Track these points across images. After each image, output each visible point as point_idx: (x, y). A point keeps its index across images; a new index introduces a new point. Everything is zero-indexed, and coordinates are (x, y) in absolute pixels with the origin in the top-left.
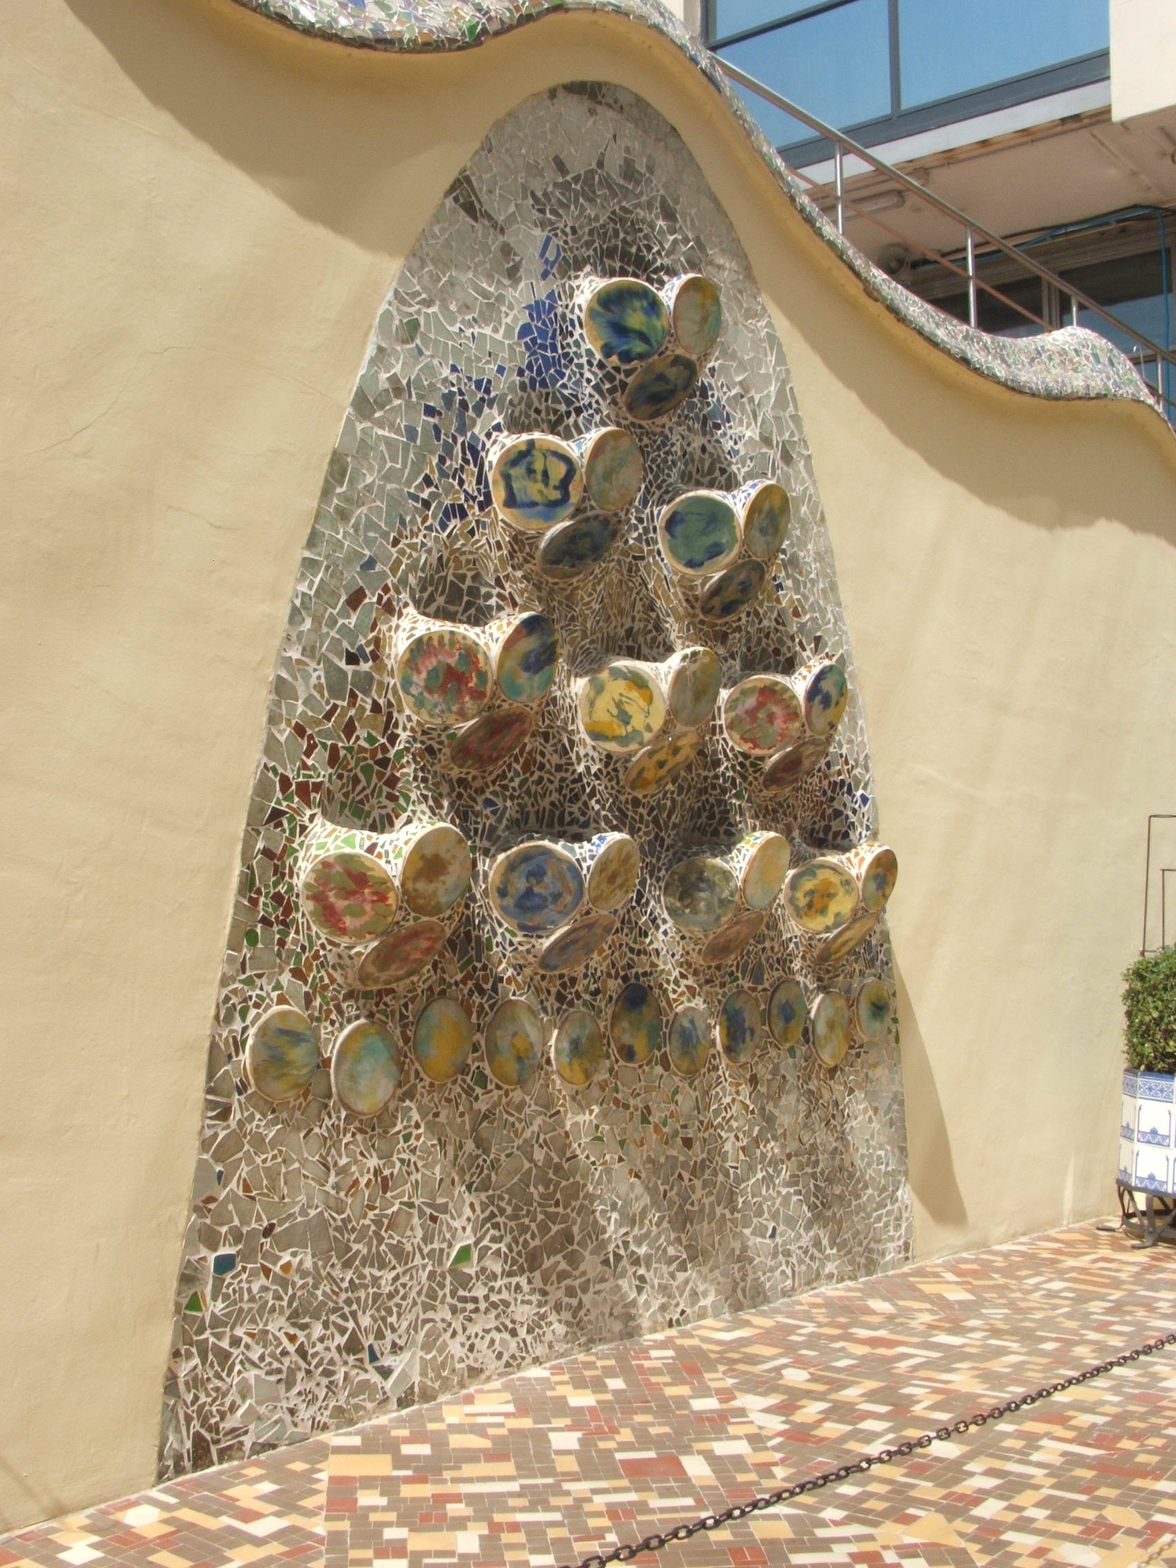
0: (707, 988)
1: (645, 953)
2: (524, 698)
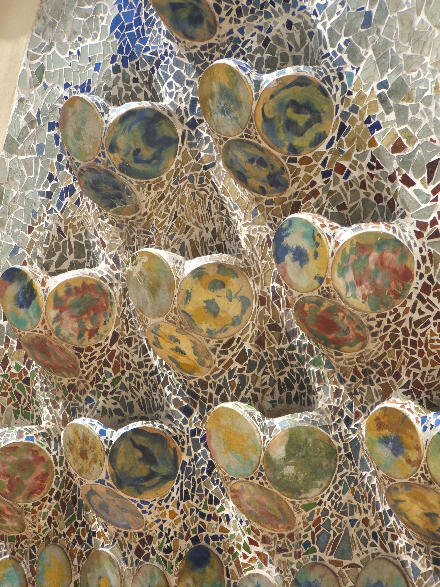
0: (279, 556)
1: (215, 518)
2: (29, 326)
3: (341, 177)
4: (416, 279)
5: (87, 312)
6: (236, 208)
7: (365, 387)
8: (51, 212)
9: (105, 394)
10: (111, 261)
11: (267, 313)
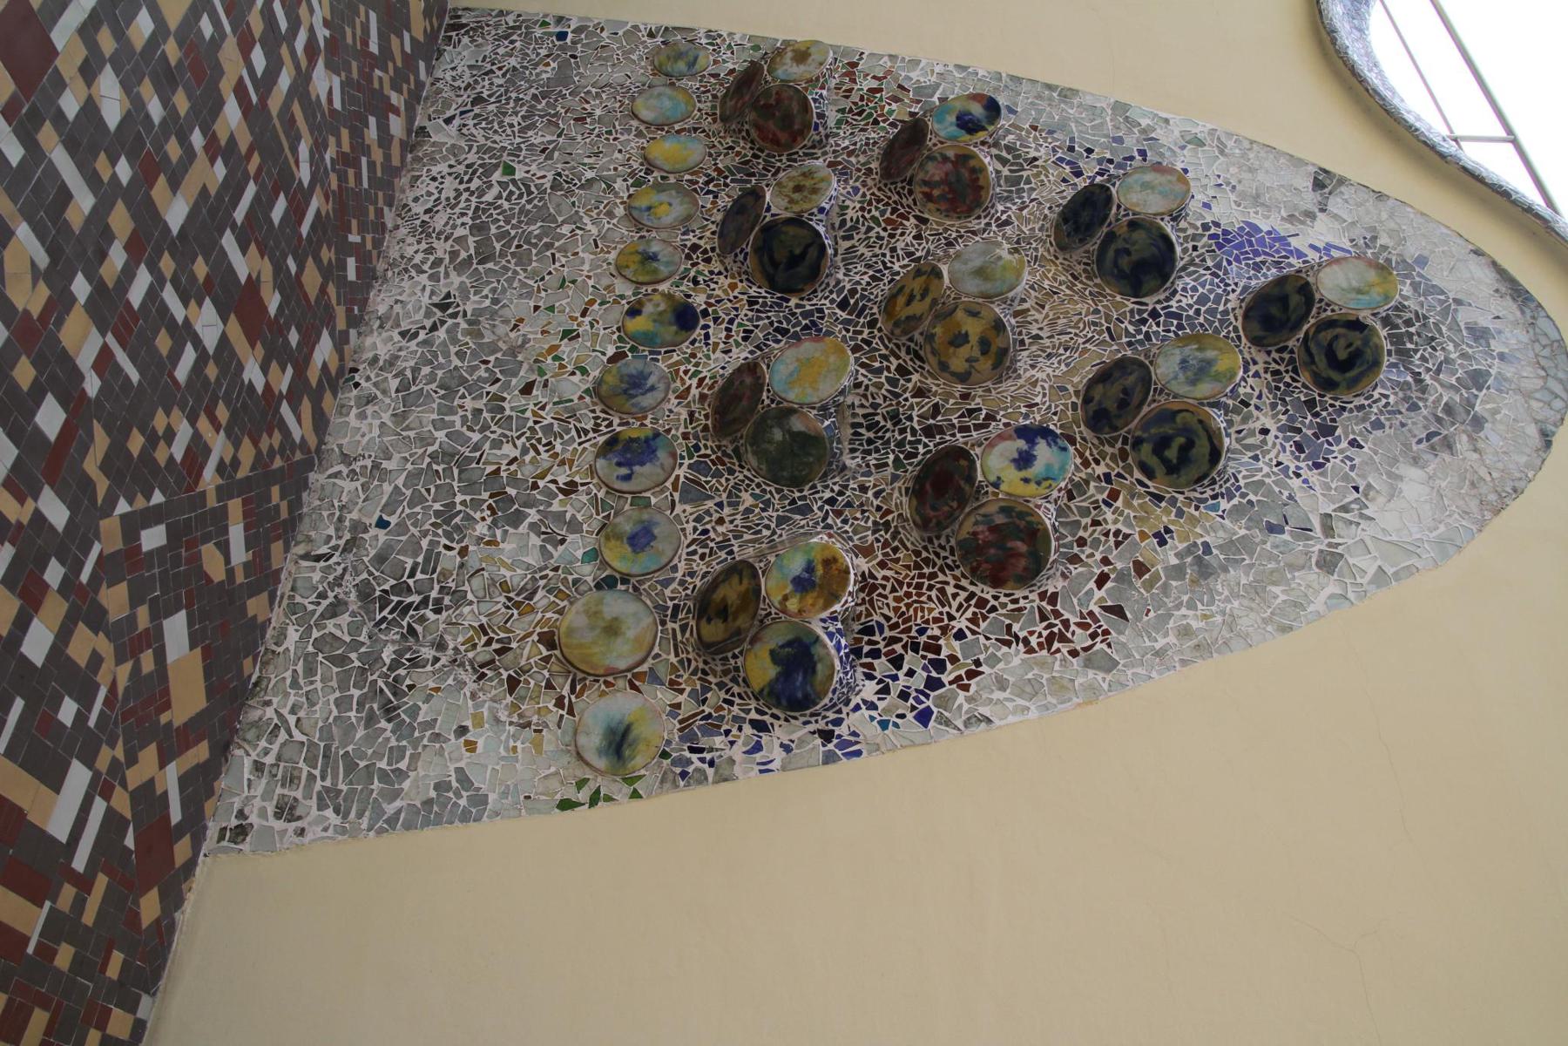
1: (728, 337)
3: (1105, 496)
4: (993, 592)
5: (952, 190)
6: (1067, 365)
7: (870, 524)
8: (1054, 150)
9: (862, 209)
10: (1004, 217)
11: (952, 401)
